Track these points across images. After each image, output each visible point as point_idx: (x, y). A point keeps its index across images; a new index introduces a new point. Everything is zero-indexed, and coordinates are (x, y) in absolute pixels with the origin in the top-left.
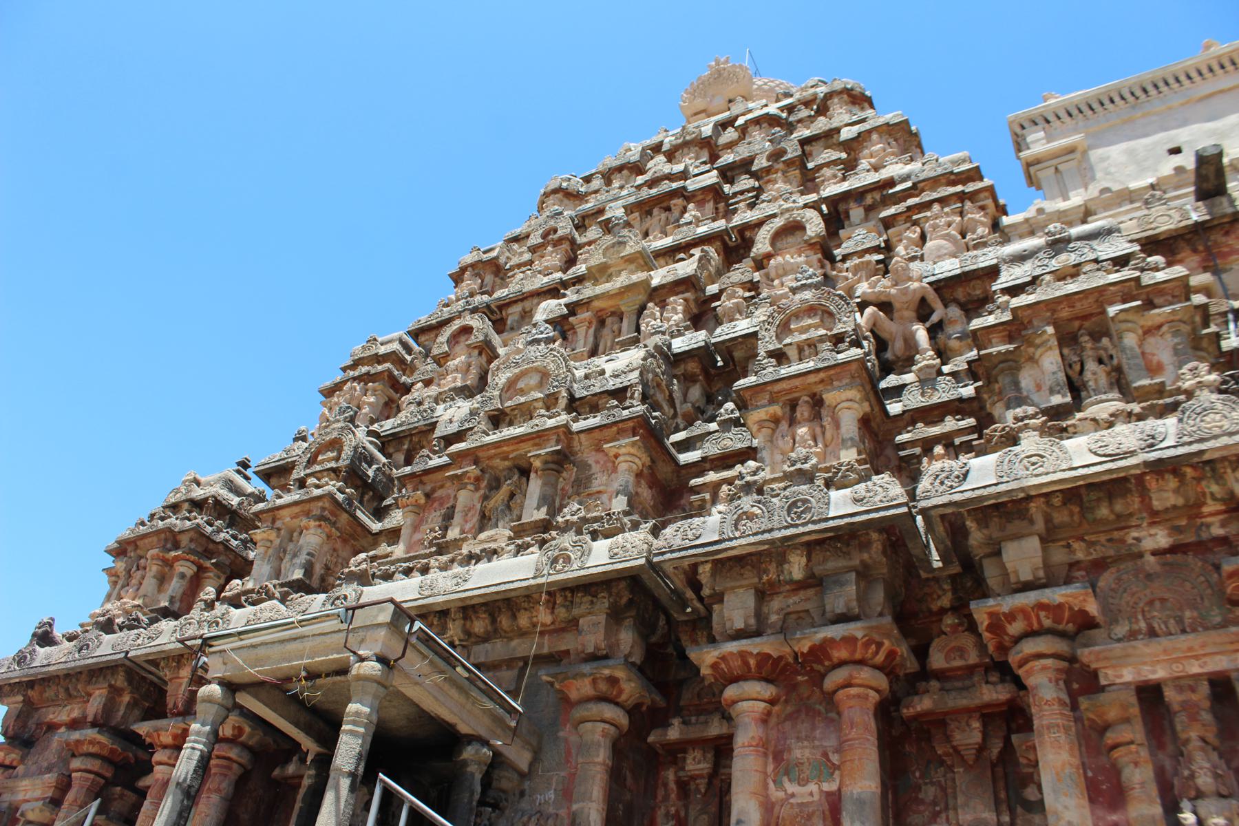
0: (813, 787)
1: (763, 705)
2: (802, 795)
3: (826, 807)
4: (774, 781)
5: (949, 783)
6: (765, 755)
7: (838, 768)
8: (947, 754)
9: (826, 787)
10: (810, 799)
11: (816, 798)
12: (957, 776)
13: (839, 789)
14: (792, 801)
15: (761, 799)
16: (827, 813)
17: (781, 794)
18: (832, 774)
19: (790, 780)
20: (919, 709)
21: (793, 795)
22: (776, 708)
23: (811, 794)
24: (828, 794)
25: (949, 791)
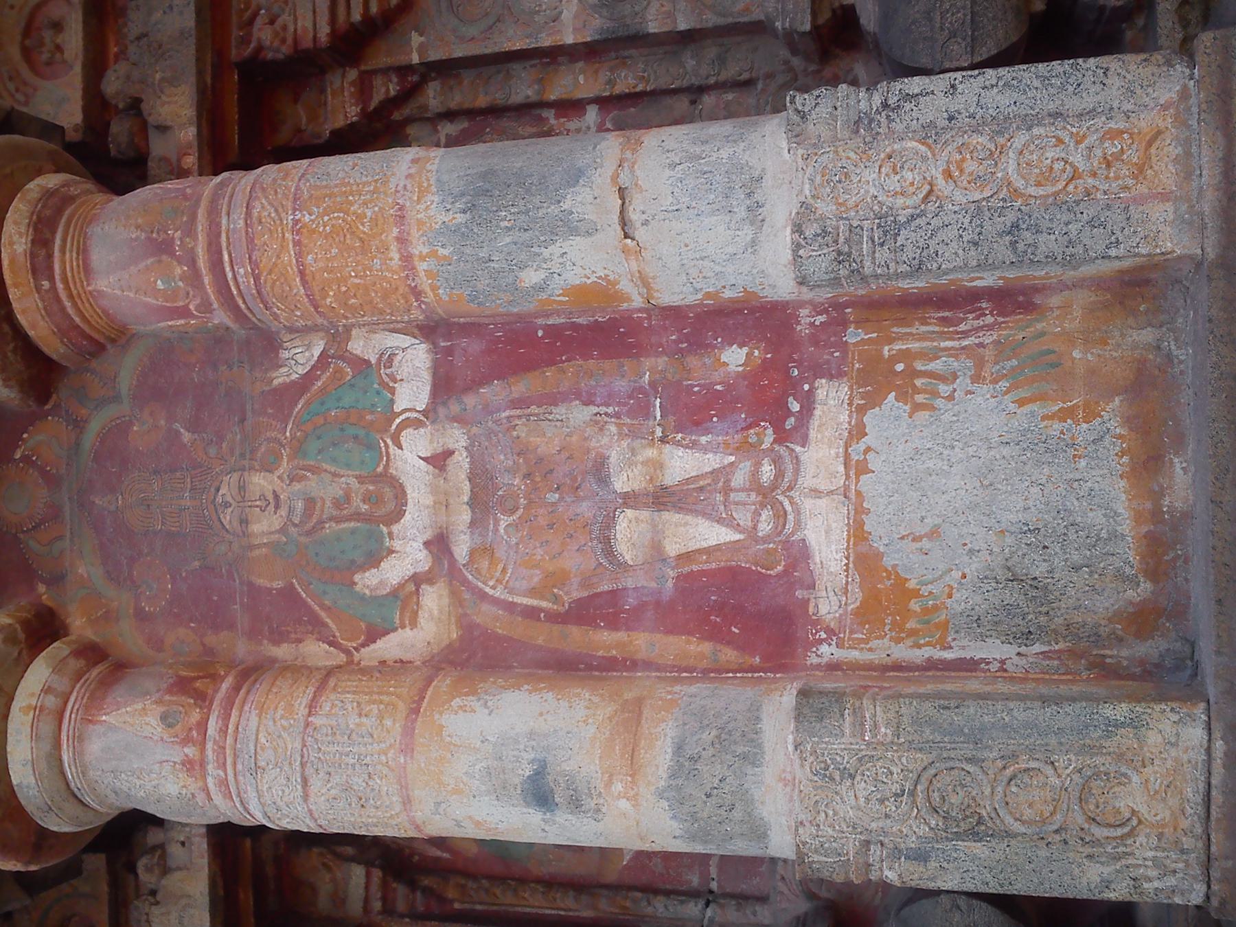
0: (409, 456)
1: (38, 674)
2: (443, 503)
3: (494, 392)
4: (373, 635)
5: (457, 100)
6: (250, 673)
7: (338, 337)
8: (364, 88)
9: (412, 394)
10: (461, 463)
11: (456, 438)
12: (434, 55)
13: (429, 330)
14: (461, 549)
15: (443, 683)
16: (522, 386)
17: (433, 600)
18: (361, 365)
19: (374, 559)
20: (189, 133)
21: (439, 544)
22: (79, 625)
23: (438, 461)
24: (445, 385)
25: (482, 101)
